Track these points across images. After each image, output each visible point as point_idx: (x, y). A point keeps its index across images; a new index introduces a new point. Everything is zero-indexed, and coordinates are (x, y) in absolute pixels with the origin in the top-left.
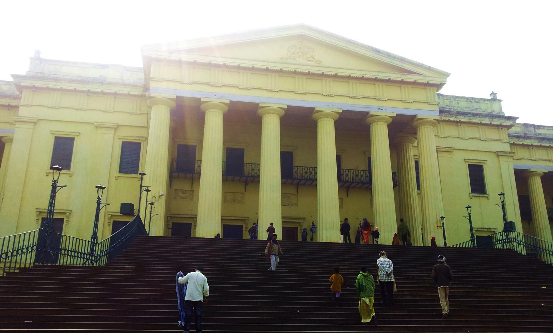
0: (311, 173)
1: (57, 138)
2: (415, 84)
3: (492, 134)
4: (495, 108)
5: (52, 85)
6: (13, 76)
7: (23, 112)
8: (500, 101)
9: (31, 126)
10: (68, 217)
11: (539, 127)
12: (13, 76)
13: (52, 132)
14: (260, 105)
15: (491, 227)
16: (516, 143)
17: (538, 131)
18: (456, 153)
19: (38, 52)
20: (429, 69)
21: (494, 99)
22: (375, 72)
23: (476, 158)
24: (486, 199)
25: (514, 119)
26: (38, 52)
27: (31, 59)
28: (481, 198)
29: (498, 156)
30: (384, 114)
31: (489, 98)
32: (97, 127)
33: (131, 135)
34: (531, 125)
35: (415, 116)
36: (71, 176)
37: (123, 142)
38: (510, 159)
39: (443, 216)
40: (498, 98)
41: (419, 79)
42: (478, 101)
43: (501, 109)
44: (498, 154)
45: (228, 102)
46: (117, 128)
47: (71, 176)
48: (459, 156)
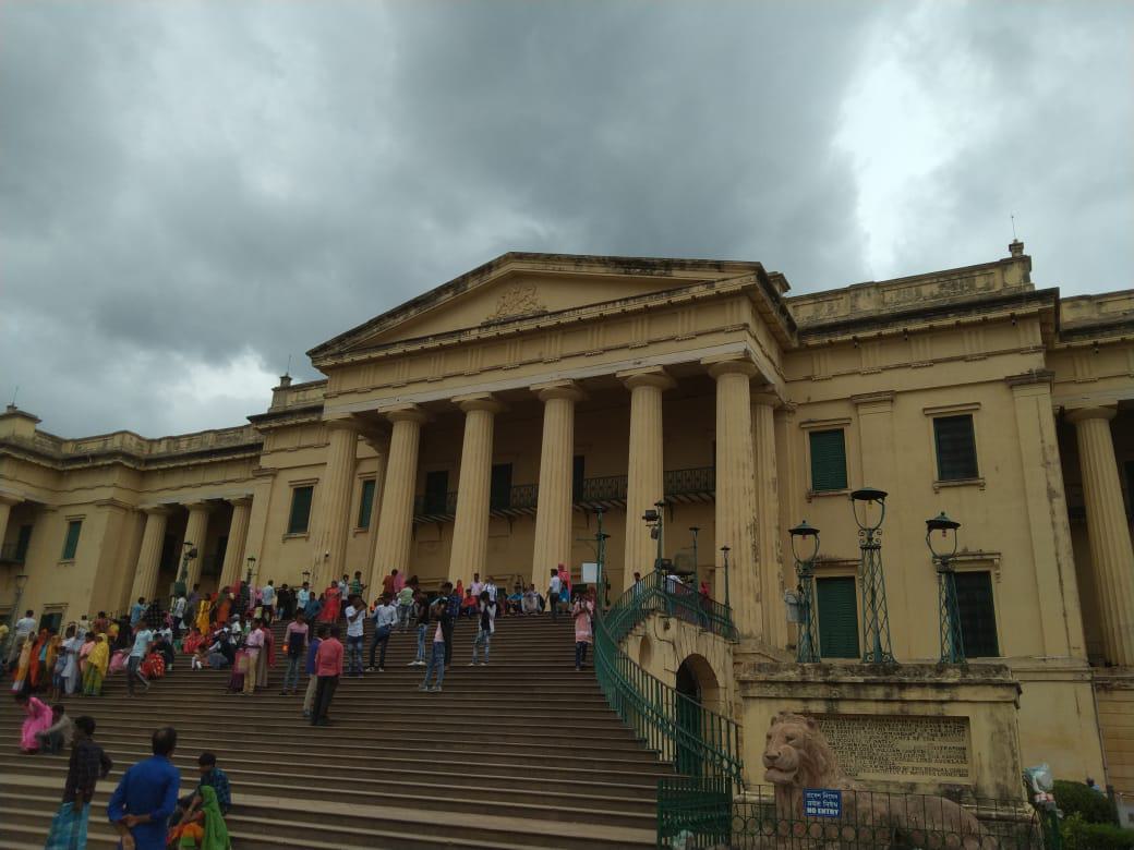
0: (698, 479)
2: (697, 304)
4: (1013, 277)
6: (249, 418)
9: (270, 480)
12: (249, 418)
15: (985, 550)
18: (902, 400)
20: (718, 266)
21: (1018, 257)
25: (1054, 292)
27: (275, 390)
28: (965, 492)
29: (1011, 387)
36: (307, 538)
38: (1044, 390)
39: (729, 546)
41: (700, 291)
43: (1026, 278)
44: (1013, 382)
48: (912, 407)
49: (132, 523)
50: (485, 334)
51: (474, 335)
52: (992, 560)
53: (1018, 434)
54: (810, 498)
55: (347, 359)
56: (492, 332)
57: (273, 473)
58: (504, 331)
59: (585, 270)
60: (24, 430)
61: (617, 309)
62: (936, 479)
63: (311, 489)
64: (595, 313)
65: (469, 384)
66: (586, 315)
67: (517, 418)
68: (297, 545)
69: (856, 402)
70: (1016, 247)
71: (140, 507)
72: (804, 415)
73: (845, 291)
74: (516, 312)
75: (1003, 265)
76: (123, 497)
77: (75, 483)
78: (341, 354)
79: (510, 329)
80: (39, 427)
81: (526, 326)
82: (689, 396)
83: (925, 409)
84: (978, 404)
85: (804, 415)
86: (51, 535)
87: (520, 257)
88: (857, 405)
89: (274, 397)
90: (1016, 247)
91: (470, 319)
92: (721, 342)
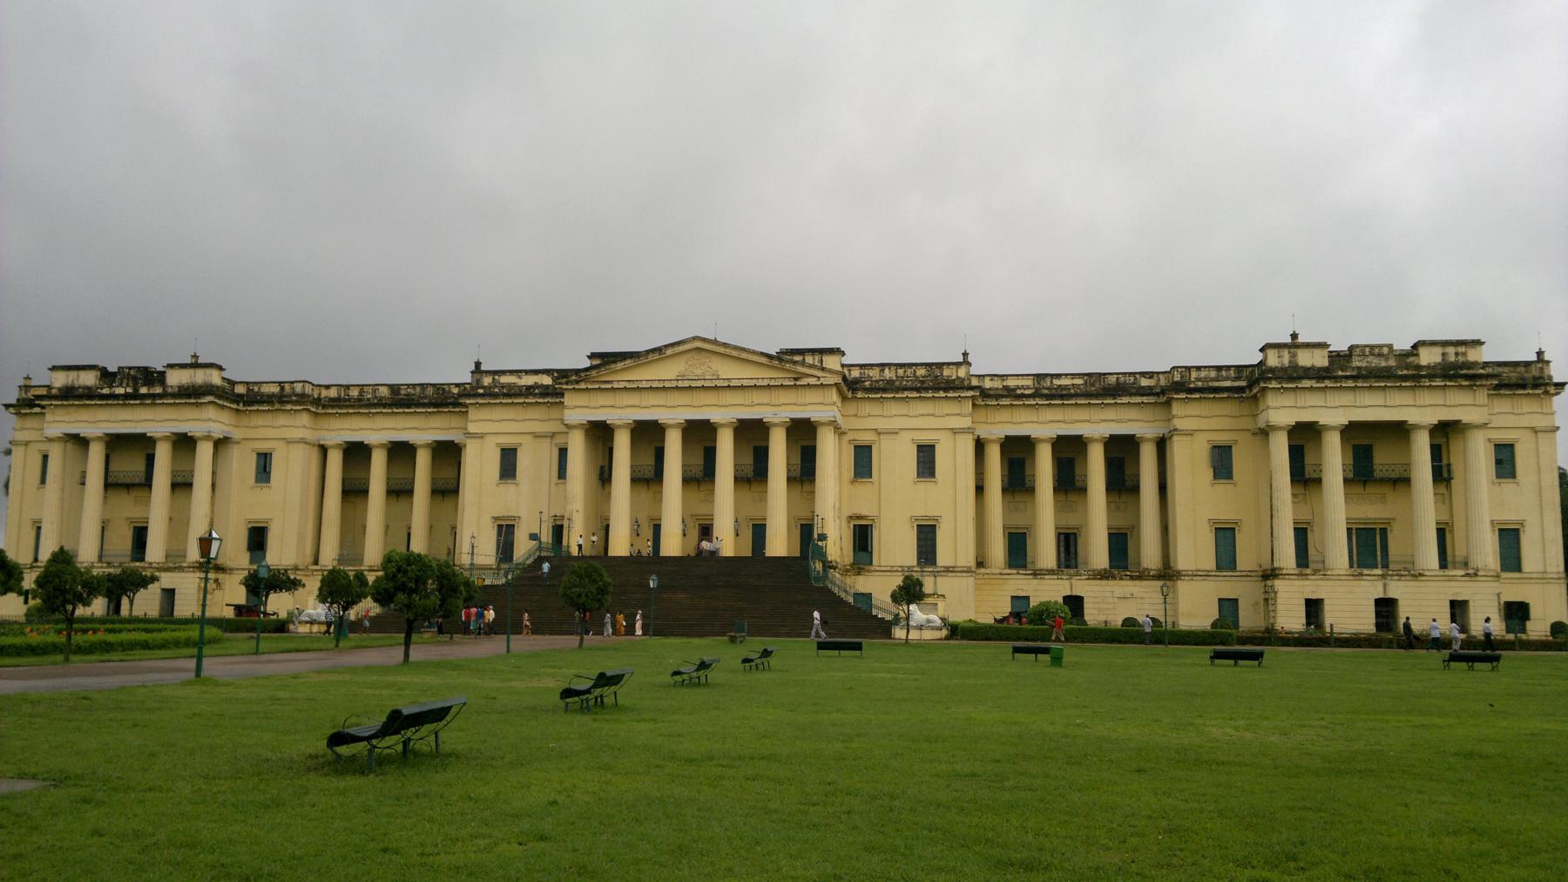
1: (503, 450)
4: (962, 373)
8: (969, 364)
11: (1059, 376)
17: (1057, 382)
19: (478, 364)
23: (925, 438)
26: (478, 364)
30: (776, 420)
34: (1046, 375)
41: (812, 381)
42: (940, 365)
46: (553, 435)
48: (906, 437)
50: (680, 384)
51: (674, 384)
53: (955, 459)
54: (852, 482)
56: (686, 384)
57: (481, 436)
58: (694, 384)
59: (744, 355)
60: (215, 378)
61: (765, 383)
64: (752, 383)
65: (673, 413)
66: (745, 383)
67: (700, 434)
68: (509, 489)
69: (878, 433)
70: (965, 354)
72: (851, 436)
74: (698, 372)
75: (958, 364)
76: (308, 435)
77: (259, 420)
78: (577, 382)
79: (699, 384)
80: (225, 374)
81: (707, 384)
82: (803, 433)
85: (851, 436)
86: (241, 464)
87: (704, 340)
90: (965, 354)
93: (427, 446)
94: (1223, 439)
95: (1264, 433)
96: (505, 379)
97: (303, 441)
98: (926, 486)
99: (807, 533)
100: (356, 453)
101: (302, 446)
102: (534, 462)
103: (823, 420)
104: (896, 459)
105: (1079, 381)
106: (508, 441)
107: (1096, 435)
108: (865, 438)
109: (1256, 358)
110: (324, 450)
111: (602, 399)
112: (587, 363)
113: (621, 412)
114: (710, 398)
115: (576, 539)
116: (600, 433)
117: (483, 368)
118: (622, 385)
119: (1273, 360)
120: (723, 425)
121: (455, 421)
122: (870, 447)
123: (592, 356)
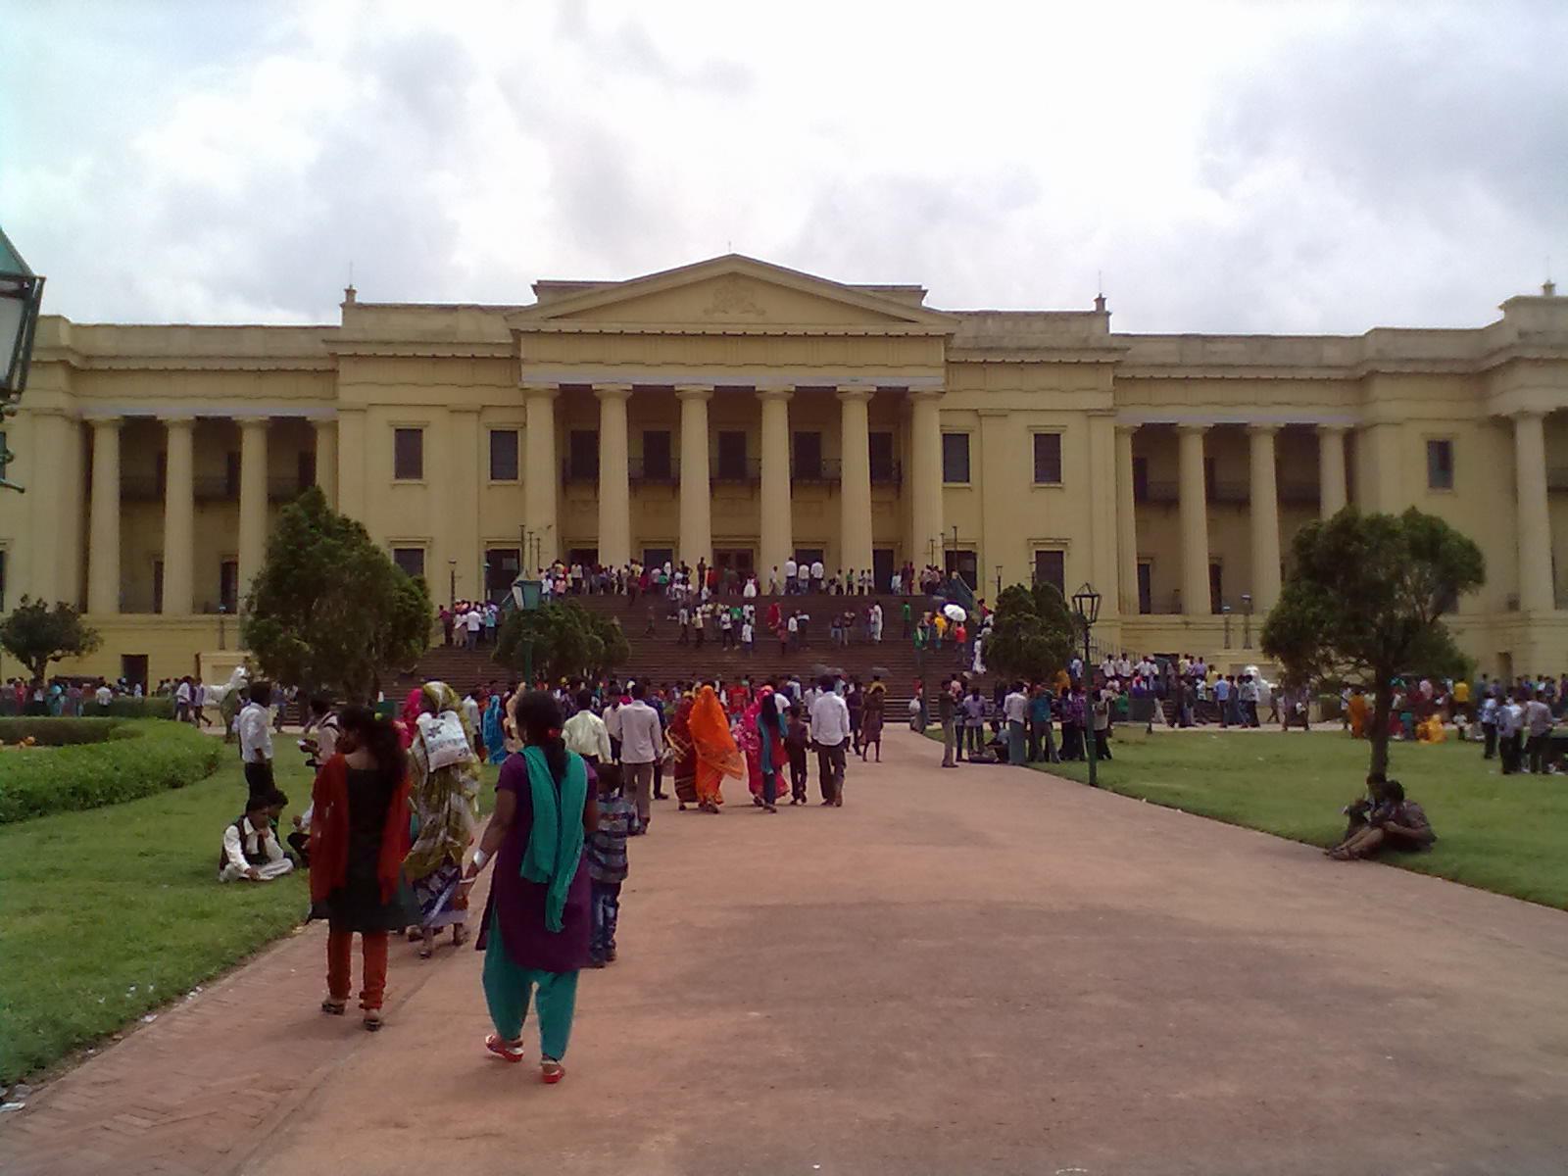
3: (1086, 378)
5: (382, 351)
7: (347, 395)
8: (1108, 314)
10: (429, 547)
13: (391, 424)
14: (677, 389)
15: (1062, 537)
16: (1156, 376)
17: (1210, 347)
19: (350, 292)
22: (844, 325)
23: (1047, 423)
24: (1058, 491)
26: (350, 292)
28: (1052, 491)
31: (1093, 308)
32: (452, 412)
33: (502, 420)
35: (907, 388)
37: (492, 432)
40: (1107, 308)
41: (912, 329)
44: (1089, 414)
45: (631, 388)
47: (425, 487)
49: (75, 437)
52: (1066, 544)
55: (553, 326)
62: (1033, 480)
63: (421, 431)
65: (695, 377)
67: (734, 412)
70: (1100, 301)
71: (87, 417)
73: (976, 314)
76: (62, 401)
83: (1029, 427)
84: (1065, 426)
88: (980, 416)
89: (344, 313)
90: (1100, 301)
91: (688, 313)
92: (918, 374)
93: (261, 425)
94: (1440, 431)
95: (1505, 426)
96: (396, 319)
97: (58, 413)
98: (1048, 495)
99: (885, 559)
100: (142, 437)
101: (59, 420)
102: (455, 450)
103: (927, 390)
104: (1005, 456)
105: (1240, 347)
106: (408, 418)
107: (1269, 424)
108: (960, 424)
109: (1500, 316)
110: (87, 431)
111: (590, 350)
112: (533, 299)
113: (613, 375)
114: (755, 352)
115: (542, 568)
116: (576, 410)
117: (358, 299)
118: (615, 328)
119: (1526, 321)
120: (774, 396)
121: (307, 386)
122: (968, 435)
123: (539, 288)
